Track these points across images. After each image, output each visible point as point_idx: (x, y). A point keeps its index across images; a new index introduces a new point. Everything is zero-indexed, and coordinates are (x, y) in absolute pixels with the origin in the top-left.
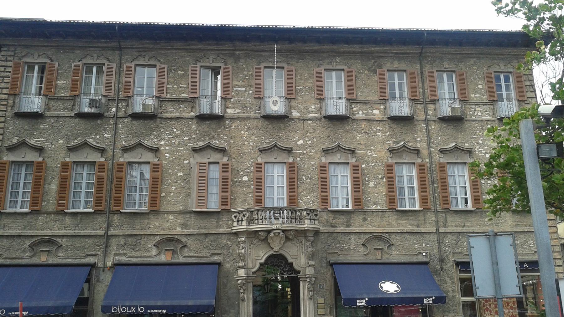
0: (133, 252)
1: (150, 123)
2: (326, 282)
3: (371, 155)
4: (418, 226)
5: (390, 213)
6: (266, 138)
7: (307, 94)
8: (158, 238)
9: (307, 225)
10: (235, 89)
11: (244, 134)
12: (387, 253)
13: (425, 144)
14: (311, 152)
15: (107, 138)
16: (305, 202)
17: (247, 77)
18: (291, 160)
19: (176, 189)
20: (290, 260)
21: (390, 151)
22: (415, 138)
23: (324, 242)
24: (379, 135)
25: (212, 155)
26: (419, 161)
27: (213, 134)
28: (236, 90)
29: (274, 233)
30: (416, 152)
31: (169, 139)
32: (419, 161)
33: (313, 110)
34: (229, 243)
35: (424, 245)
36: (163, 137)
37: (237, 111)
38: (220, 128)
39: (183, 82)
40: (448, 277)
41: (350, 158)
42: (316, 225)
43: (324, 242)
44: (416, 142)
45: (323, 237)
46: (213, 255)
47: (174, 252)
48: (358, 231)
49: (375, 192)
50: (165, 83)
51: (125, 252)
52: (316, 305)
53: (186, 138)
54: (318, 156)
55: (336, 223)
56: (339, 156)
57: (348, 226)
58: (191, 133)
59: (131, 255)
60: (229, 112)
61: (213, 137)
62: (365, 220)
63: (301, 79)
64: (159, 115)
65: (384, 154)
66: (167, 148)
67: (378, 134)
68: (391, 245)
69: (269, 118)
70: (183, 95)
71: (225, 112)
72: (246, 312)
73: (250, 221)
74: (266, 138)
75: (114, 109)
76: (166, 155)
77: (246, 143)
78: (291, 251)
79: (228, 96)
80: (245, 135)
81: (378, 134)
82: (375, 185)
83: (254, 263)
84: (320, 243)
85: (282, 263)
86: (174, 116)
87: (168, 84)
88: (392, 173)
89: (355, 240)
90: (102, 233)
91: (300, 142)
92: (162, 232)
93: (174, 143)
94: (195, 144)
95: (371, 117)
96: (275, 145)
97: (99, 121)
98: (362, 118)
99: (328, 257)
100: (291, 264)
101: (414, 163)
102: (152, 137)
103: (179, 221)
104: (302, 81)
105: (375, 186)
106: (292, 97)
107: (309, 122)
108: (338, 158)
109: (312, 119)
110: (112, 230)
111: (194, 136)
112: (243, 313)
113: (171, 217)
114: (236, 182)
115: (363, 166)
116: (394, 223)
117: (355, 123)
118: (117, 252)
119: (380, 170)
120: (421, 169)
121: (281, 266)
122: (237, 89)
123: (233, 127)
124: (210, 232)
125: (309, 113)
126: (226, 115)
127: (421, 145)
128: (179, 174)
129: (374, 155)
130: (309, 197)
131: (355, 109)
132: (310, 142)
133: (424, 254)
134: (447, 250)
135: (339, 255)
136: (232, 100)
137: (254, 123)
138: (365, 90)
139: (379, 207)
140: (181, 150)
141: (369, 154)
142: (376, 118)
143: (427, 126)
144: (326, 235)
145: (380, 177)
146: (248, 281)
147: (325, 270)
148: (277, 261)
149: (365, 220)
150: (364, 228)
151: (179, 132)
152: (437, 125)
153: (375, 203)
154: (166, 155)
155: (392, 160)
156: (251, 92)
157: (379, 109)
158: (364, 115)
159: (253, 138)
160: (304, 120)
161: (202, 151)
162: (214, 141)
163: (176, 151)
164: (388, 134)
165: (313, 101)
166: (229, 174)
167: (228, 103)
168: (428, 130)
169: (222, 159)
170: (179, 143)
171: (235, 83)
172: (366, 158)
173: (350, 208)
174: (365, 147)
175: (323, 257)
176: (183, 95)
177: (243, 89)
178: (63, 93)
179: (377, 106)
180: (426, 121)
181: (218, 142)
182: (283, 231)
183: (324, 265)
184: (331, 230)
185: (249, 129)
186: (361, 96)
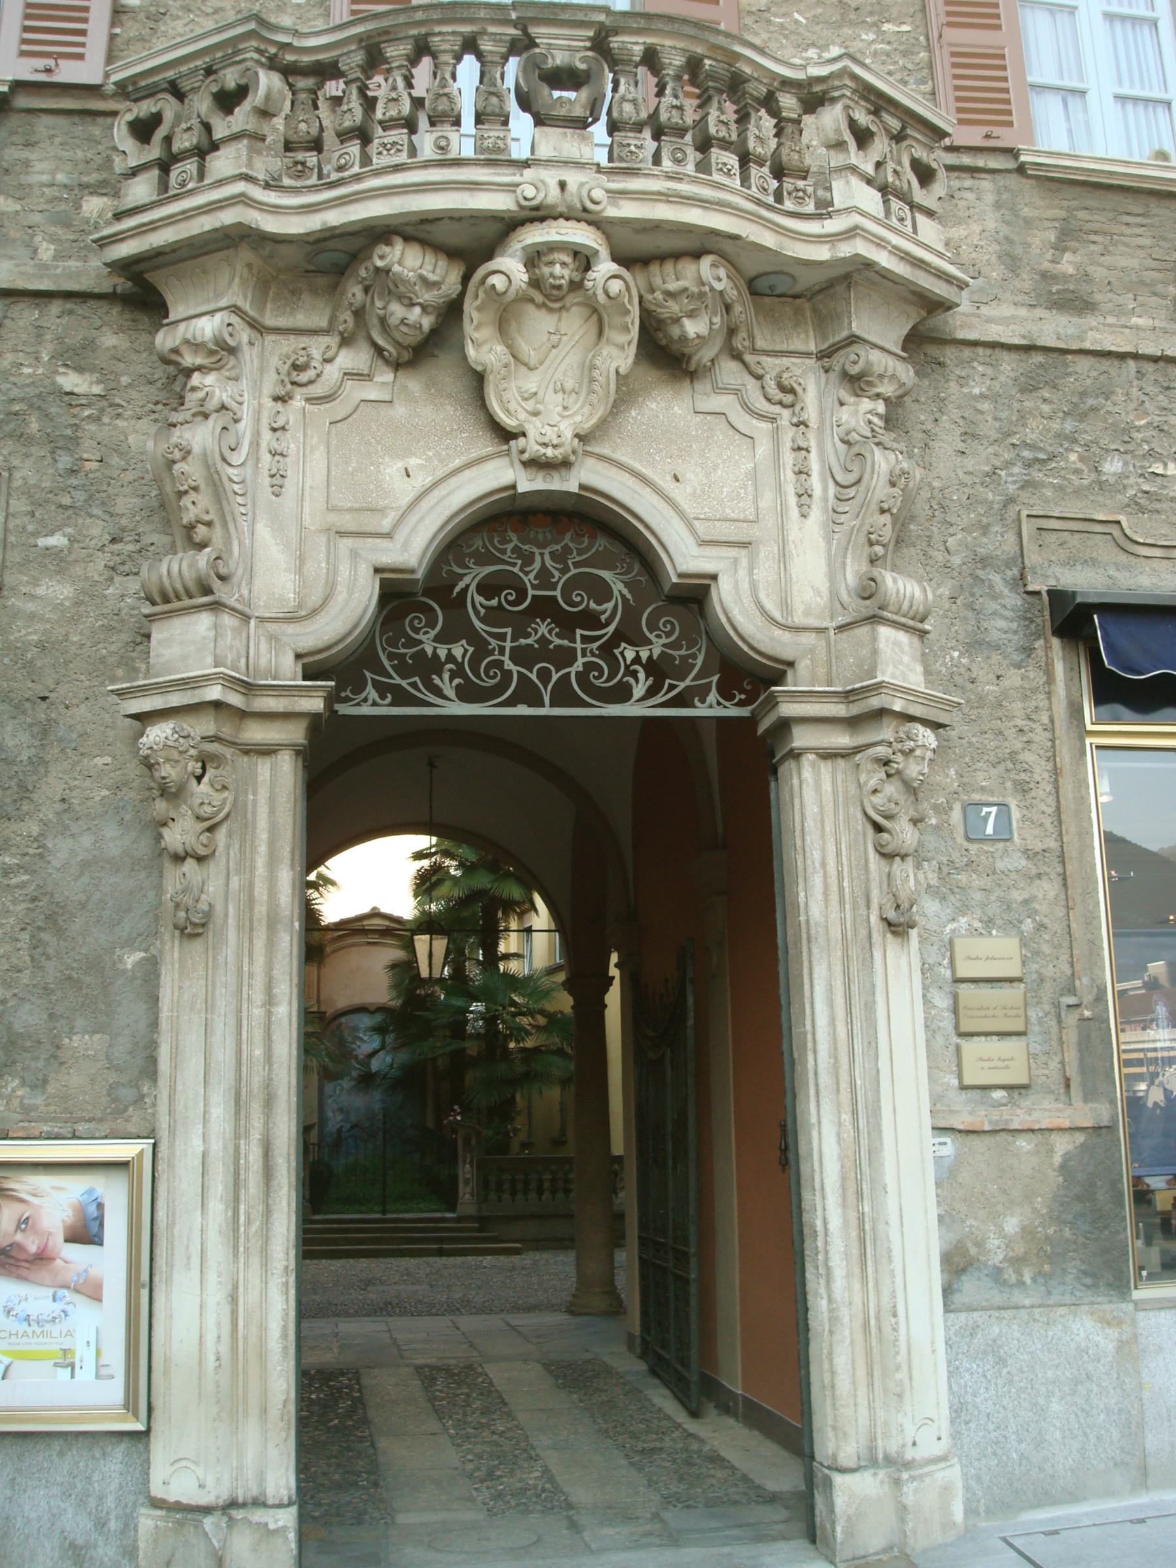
2: (1022, 788)
20: (684, 556)
23: (989, 428)
29: (534, 258)
34: (70, 381)
43: (989, 428)
52: (942, 1001)
72: (224, 1055)
78: (693, 476)
83: (317, 565)
84: (948, 440)
85: (602, 592)
99: (1033, 557)
100: (694, 597)
112: (193, 1066)
135: (1126, 544)
144: (1009, 365)
146: (257, 733)
147: (1013, 679)
175: (984, 562)
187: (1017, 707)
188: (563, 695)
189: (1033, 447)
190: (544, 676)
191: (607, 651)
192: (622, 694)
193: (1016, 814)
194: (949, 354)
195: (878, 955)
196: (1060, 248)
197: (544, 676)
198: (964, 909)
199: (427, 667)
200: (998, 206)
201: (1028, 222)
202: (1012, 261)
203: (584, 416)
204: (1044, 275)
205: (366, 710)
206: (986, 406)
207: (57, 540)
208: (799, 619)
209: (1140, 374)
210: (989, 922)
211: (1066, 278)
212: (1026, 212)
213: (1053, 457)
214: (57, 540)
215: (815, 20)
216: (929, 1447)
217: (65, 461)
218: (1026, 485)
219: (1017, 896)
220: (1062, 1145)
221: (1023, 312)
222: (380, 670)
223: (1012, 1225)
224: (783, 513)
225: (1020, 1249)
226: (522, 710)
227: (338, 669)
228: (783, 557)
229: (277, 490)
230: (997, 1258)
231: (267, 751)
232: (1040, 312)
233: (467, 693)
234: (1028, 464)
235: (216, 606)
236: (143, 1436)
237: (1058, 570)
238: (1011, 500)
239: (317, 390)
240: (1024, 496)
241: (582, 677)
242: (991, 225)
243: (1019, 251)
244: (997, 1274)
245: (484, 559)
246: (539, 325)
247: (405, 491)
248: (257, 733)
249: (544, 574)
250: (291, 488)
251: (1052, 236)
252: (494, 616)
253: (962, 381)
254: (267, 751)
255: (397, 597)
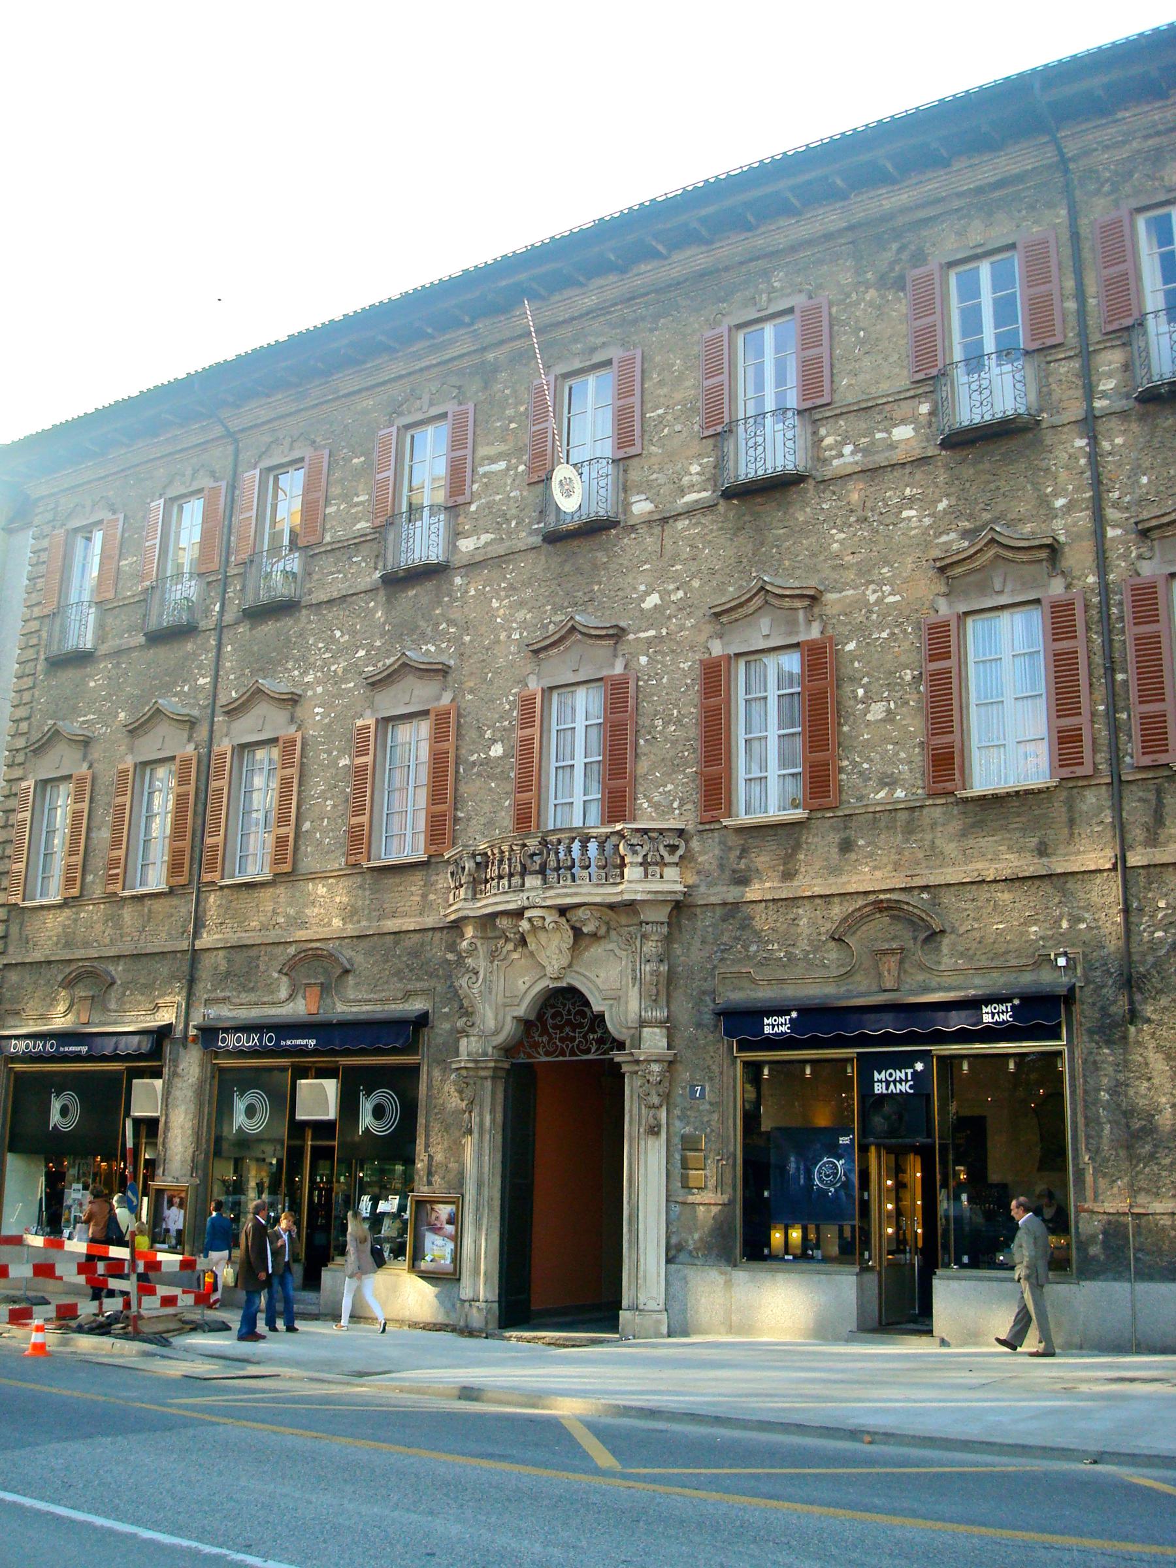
0: (243, 995)
1: (287, 623)
2: (711, 1079)
3: (877, 602)
4: (1043, 850)
5: (937, 813)
6: (555, 610)
7: (678, 428)
8: (292, 950)
9: (634, 883)
10: (481, 470)
11: (498, 609)
12: (922, 967)
13: (1083, 518)
14: (682, 628)
15: (202, 687)
16: (656, 806)
17: (513, 426)
18: (618, 669)
19: (334, 806)
21: (942, 570)
22: (1044, 502)
23: (710, 939)
24: (909, 519)
25: (416, 692)
26: (1056, 588)
27: (422, 624)
28: (485, 475)
30: (1044, 554)
31: (326, 662)
32: (1056, 588)
33: (695, 478)
34: (450, 956)
35: (1065, 924)
36: (312, 660)
37: (486, 537)
38: (439, 603)
39: (361, 487)
40: (1159, 1049)
41: (802, 628)
42: (672, 881)
43: (710, 939)
44: (1052, 514)
45: (705, 921)
46: (408, 995)
47: (325, 989)
48: (818, 891)
49: (887, 740)
50: (322, 503)
51: (229, 994)
52: (678, 1157)
53: (361, 653)
54: (702, 638)
55: (749, 869)
56: (765, 623)
57: (788, 876)
58: (372, 635)
59: (237, 1001)
60: (464, 549)
61: (423, 634)
62: (846, 846)
63: (661, 383)
64: (305, 600)
65: (927, 588)
66: (319, 690)
67: (905, 514)
68: (934, 934)
69: (554, 538)
70: (358, 526)
71: (455, 546)
73: (477, 884)
74: (555, 610)
75: (217, 608)
76: (317, 710)
77: (503, 636)
78: (603, 975)
79: (460, 499)
80: (501, 612)
81: (905, 514)
82: (889, 711)
84: (697, 943)
86: (335, 595)
87: (327, 503)
88: (947, 656)
89: (812, 923)
90: (184, 945)
91: (653, 600)
92: (301, 935)
93: (335, 671)
94: (380, 665)
95: (881, 459)
96: (573, 628)
97: (190, 647)
98: (849, 471)
100: (600, 1017)
101: (1037, 601)
102: (290, 665)
103: (338, 899)
104: (665, 390)
105: (890, 716)
106: (632, 451)
107: (681, 524)
108: (762, 631)
109: (689, 512)
110: (205, 935)
111: (378, 643)
113: (322, 890)
114: (474, 763)
115: (851, 646)
116: (951, 848)
117: (828, 495)
118: (213, 995)
119: (905, 653)
120: (1061, 620)
121: (581, 1026)
122: (487, 468)
123: (473, 592)
124: (404, 928)
125: (682, 492)
126: (457, 561)
127: (1068, 524)
128: (342, 763)
129: (891, 599)
130: (670, 787)
131: (829, 441)
132: (680, 594)
133: (1062, 962)
134: (1161, 941)
135: (754, 981)
136: (473, 508)
137: (524, 564)
138: (866, 362)
139: (900, 794)
140: (350, 690)
141: (872, 598)
142: (898, 456)
143: (1094, 440)
145: (908, 678)
146: (482, 1073)
147: (711, 1037)
148: (564, 1009)
149: (846, 846)
150: (844, 879)
151: (347, 637)
152: (1135, 427)
153: (889, 781)
154: (317, 710)
155: (950, 604)
156: (521, 468)
157: (913, 419)
158: (858, 457)
159: (521, 615)
160: (664, 520)
161: (393, 682)
162: (424, 648)
163: (340, 696)
164: (941, 506)
165: (695, 447)
166: (449, 746)
167: (461, 519)
168: (1094, 457)
169: (438, 698)
170: (345, 670)
171: (483, 451)
172: (859, 617)
173: (800, 814)
174: (860, 573)
175: (704, 993)
176: (358, 526)
177: (502, 465)
178: (130, 589)
179: (905, 408)
180: (1090, 424)
181: (433, 649)
182: (563, 911)
183: (708, 1018)
184: (732, 894)
185: (512, 588)
186: (848, 387)
187: (711, 1049)
188: (573, 1053)
189: (725, 944)
190: (567, 1046)
191: (585, 1037)
192: (588, 1051)
193: (707, 1089)
194: (698, 910)
195: (642, 1142)
196: (740, 857)
197: (567, 1046)
198: (688, 1124)
199: (536, 1045)
200: (720, 843)
201: (730, 849)
202: (721, 867)
203: (565, 962)
204: (734, 871)
205: (521, 1061)
206: (710, 929)
207: (446, 1010)
208: (630, 1025)
209: (766, 908)
210: (696, 1129)
211: (741, 871)
212: (730, 844)
213: (731, 947)
214: (446, 1010)
215: (662, 775)
216: (651, 1305)
217: (449, 983)
218: (722, 960)
219: (705, 1119)
220: (715, 1210)
221: (725, 888)
222: (524, 1046)
223: (696, 1236)
224: (627, 985)
225: (698, 1245)
226: (561, 1058)
227: (508, 1050)
228: (627, 1003)
229: (490, 993)
230: (691, 1248)
231: (486, 1078)
232: (732, 888)
233: (547, 1054)
234: (723, 951)
235: (467, 1036)
236: (459, 1279)
237: (728, 994)
238: (715, 967)
239: (501, 957)
240: (720, 965)
241: (578, 1046)
242: (717, 852)
243: (725, 862)
244: (690, 1252)
245: (553, 1006)
246: (542, 936)
247: (523, 988)
248: (482, 1073)
249: (569, 1010)
250: (494, 992)
251: (738, 853)
252: (555, 1027)
253: (703, 920)
254: (486, 1078)
255: (526, 1025)
